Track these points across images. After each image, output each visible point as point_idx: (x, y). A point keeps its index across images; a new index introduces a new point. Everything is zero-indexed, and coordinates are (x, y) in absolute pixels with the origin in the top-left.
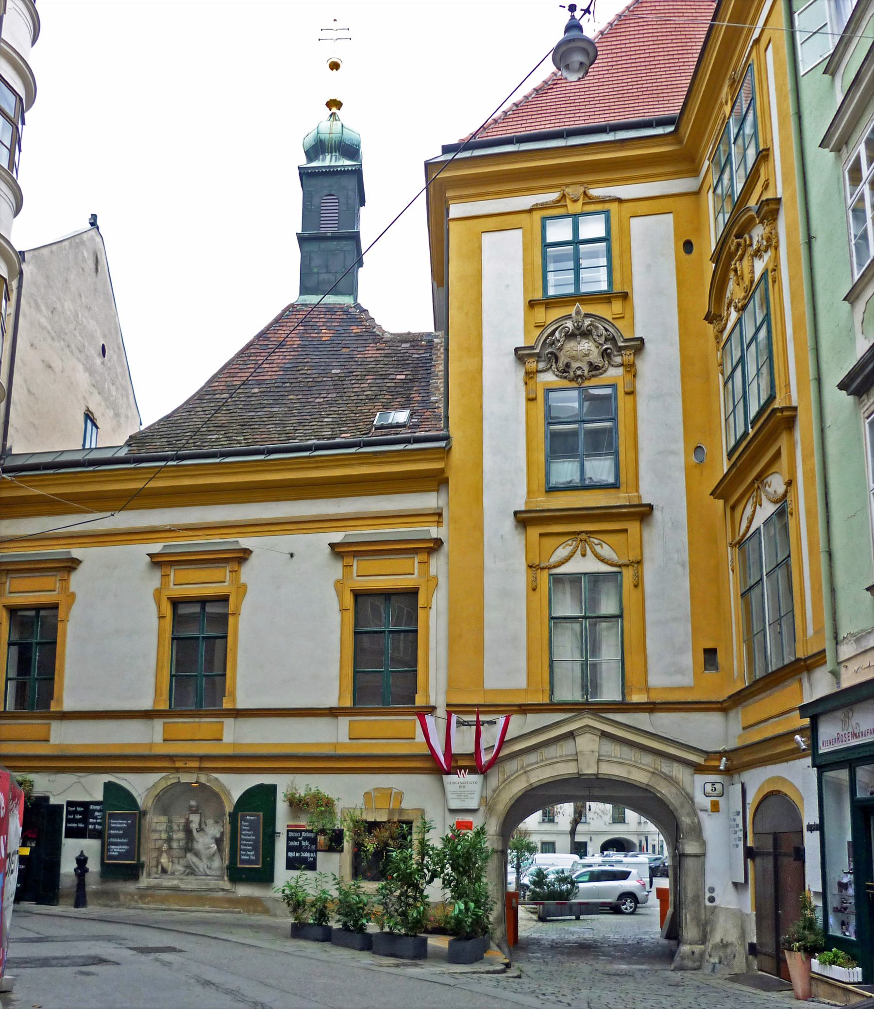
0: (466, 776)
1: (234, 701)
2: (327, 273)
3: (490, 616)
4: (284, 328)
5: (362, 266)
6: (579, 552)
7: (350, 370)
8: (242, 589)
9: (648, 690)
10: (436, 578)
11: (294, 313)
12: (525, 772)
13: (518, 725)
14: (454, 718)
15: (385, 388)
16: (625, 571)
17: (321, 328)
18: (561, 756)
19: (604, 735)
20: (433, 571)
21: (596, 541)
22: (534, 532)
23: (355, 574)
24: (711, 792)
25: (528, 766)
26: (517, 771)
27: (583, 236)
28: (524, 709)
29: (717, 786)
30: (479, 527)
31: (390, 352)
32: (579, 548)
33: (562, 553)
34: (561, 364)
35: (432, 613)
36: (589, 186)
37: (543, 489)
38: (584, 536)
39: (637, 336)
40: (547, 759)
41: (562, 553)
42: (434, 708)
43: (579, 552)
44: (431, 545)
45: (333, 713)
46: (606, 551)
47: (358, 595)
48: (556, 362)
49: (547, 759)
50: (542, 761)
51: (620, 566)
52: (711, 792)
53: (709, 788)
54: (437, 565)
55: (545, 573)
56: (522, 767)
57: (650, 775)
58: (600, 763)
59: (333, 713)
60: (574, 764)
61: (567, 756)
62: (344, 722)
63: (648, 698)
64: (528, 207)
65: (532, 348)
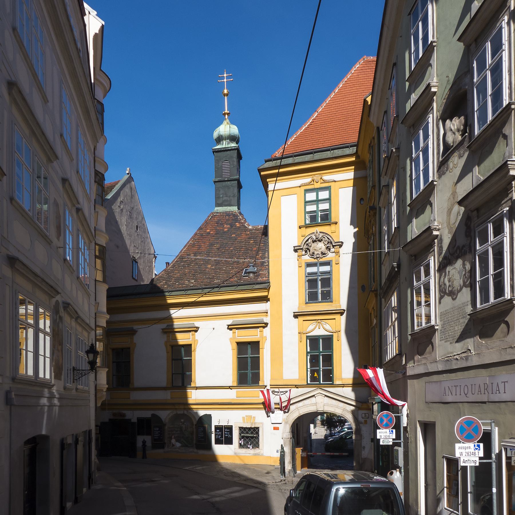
0: (277, 411)
1: (195, 383)
2: (226, 196)
3: (285, 352)
4: (209, 225)
5: (242, 188)
6: (317, 327)
7: (235, 246)
8: (196, 341)
9: (342, 379)
10: (266, 337)
11: (213, 217)
12: (298, 410)
13: (295, 392)
14: (270, 392)
15: (248, 255)
16: (334, 334)
17: (224, 224)
18: (311, 404)
19: (326, 396)
20: (264, 335)
21: (324, 323)
22: (301, 319)
23: (237, 336)
24: (364, 417)
25: (299, 407)
26: (295, 409)
27: (320, 198)
28: (297, 386)
29: (367, 415)
30: (280, 318)
31: (251, 236)
32: (318, 326)
33: (311, 327)
34: (311, 253)
35: (265, 350)
36: (323, 175)
37: (304, 303)
38: (319, 321)
39: (340, 241)
40: (306, 405)
41: (311, 327)
42: (266, 386)
43: (317, 327)
44: (264, 325)
45: (230, 388)
46: (328, 327)
47: (238, 344)
48: (309, 252)
49: (306, 405)
50: (304, 406)
51: (333, 333)
52: (364, 417)
53: (363, 415)
54: (267, 331)
55: (305, 335)
56: (297, 408)
57: (342, 411)
58: (324, 406)
59: (230, 388)
60: (315, 406)
61: (313, 404)
62: (234, 391)
63: (342, 382)
64: (299, 186)
65: (300, 246)
